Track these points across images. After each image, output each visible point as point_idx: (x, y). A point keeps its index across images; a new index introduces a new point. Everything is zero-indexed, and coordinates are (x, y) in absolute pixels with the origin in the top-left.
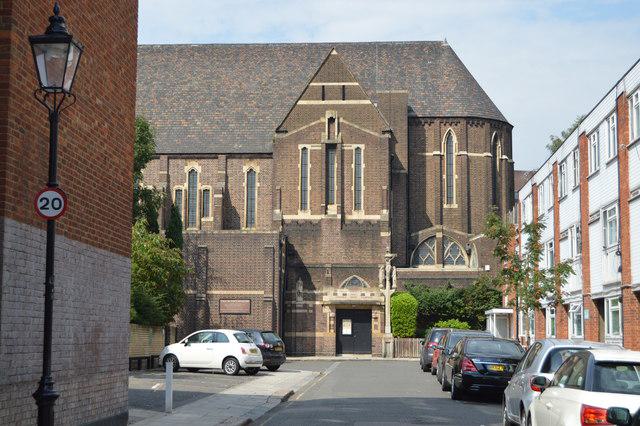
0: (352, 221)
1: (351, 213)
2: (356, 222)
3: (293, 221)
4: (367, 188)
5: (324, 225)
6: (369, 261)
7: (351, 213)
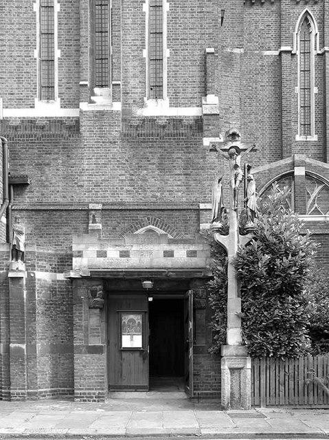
0: (145, 120)
1: (142, 105)
2: (152, 120)
3: (23, 120)
4: (175, 52)
5: (84, 123)
6: (180, 197)
7: (142, 105)
